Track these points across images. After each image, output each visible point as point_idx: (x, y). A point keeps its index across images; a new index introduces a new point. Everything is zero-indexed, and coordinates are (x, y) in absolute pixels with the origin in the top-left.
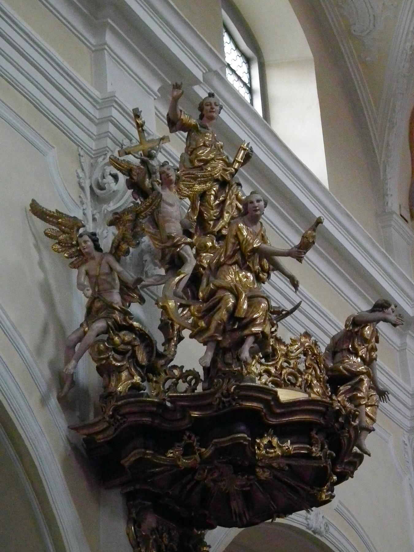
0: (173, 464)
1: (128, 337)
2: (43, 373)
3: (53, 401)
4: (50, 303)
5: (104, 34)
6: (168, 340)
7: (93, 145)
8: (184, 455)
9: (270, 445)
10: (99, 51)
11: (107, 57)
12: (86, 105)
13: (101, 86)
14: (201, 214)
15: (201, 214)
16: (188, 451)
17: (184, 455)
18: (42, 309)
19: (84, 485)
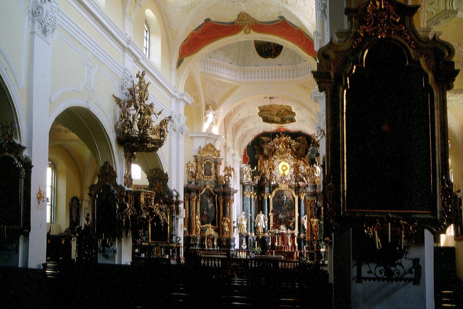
0: (134, 146)
1: (128, 123)
2: (113, 126)
3: (114, 131)
4: (114, 112)
5: (125, 53)
6: (133, 121)
7: (121, 77)
8: (136, 145)
9: (150, 145)
10: (124, 56)
11: (125, 58)
12: (121, 69)
13: (124, 66)
14: (141, 97)
15: (141, 97)
16: (136, 144)
17: (136, 145)
18: (113, 114)
19: (118, 145)
